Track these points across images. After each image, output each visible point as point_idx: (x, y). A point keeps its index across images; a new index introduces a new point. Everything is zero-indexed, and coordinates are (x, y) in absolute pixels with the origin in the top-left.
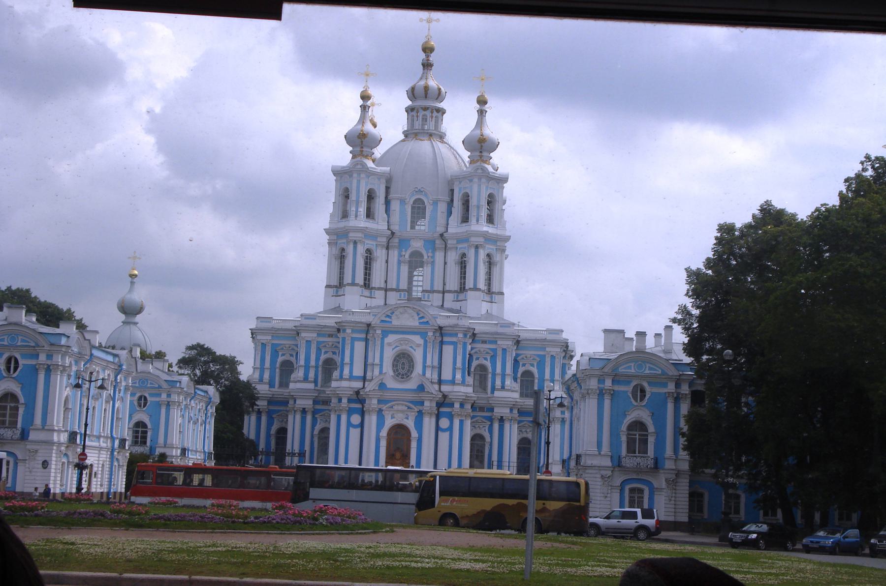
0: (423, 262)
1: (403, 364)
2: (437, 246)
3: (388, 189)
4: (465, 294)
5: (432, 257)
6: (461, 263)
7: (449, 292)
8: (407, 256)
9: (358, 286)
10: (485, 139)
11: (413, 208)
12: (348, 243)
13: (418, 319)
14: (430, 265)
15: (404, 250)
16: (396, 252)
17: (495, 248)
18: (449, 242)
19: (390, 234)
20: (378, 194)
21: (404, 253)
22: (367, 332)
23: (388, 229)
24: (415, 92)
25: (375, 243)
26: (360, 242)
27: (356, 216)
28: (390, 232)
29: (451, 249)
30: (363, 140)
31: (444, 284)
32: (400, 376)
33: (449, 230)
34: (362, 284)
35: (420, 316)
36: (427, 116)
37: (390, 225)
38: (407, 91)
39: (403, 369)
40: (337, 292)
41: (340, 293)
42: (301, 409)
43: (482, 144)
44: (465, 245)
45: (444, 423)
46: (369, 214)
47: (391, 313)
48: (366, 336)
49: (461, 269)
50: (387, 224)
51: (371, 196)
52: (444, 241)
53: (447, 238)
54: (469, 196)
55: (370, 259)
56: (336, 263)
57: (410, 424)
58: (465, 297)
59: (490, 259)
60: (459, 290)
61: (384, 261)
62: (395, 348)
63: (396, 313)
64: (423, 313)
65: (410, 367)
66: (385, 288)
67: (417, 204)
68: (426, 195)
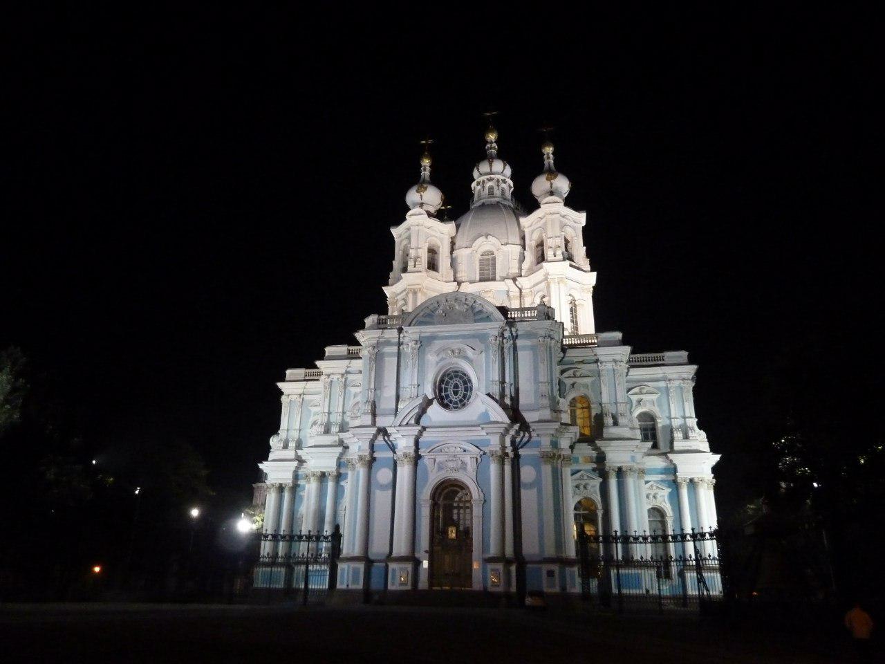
1: (456, 386)
2: (511, 294)
3: (453, 244)
11: (480, 260)
22: (400, 344)
32: (451, 405)
39: (456, 393)
42: (319, 474)
45: (527, 473)
46: (433, 266)
48: (399, 349)
51: (432, 251)
52: (518, 287)
57: (468, 478)
62: (441, 360)
65: (466, 389)
68: (493, 244)
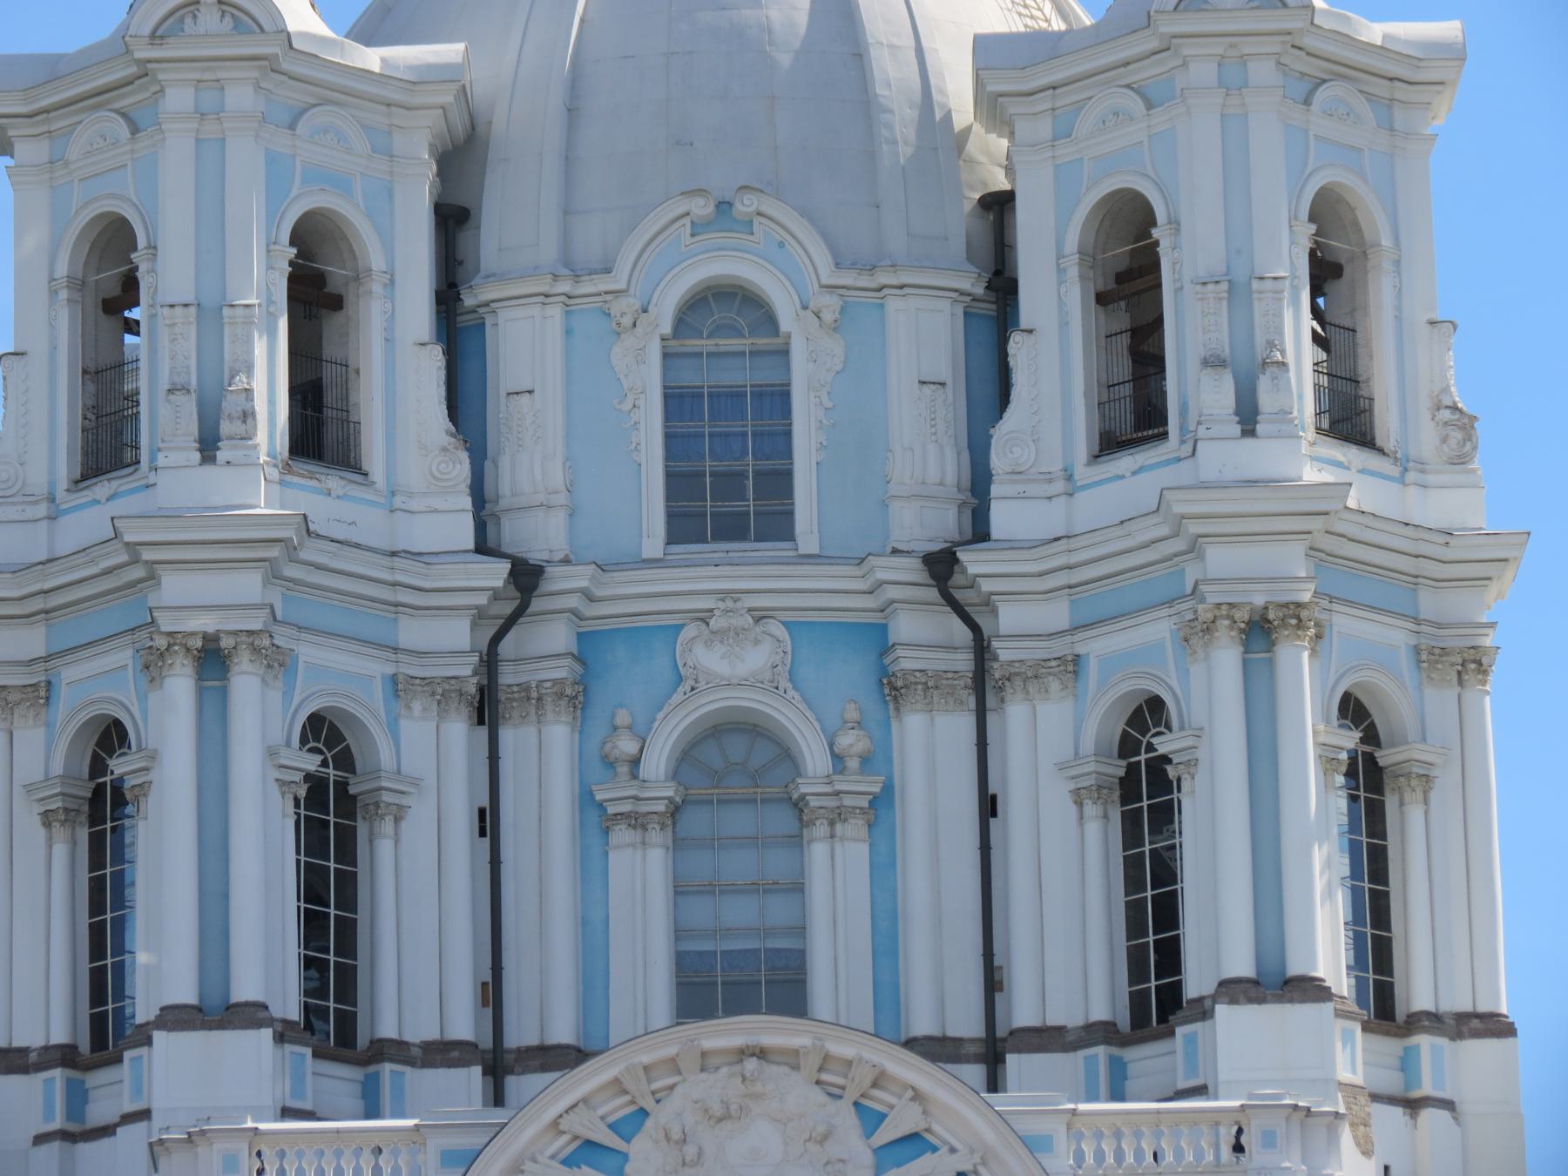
0: (798, 806)
4: (1191, 1040)
5: (865, 760)
6: (1128, 788)
7: (1046, 1038)
8: (657, 762)
9: (258, 1024)
12: (153, 664)
13: (868, 1158)
14: (854, 828)
15: (622, 718)
16: (559, 734)
17: (1397, 636)
18: (1010, 618)
19: (499, 583)
20: (377, 261)
21: (628, 746)
23: (483, 547)
25: (377, 668)
26: (256, 650)
27: (208, 447)
28: (504, 567)
29: (1034, 674)
31: (993, 982)
33: (1002, 518)
34: (294, 1013)
35: (886, 1134)
37: (496, 517)
40: (77, 1099)
41: (100, 1111)
44: (1158, 629)
47: (611, 1127)
49: (1131, 836)
50: (467, 502)
53: (986, 586)
54: (1153, 223)
55: (348, 804)
56: (60, 852)
58: (1192, 1068)
59: (1371, 736)
60: (1124, 1022)
61: (461, 823)
63: (662, 1116)
64: (918, 1096)
66: (487, 1042)
67: (716, 332)
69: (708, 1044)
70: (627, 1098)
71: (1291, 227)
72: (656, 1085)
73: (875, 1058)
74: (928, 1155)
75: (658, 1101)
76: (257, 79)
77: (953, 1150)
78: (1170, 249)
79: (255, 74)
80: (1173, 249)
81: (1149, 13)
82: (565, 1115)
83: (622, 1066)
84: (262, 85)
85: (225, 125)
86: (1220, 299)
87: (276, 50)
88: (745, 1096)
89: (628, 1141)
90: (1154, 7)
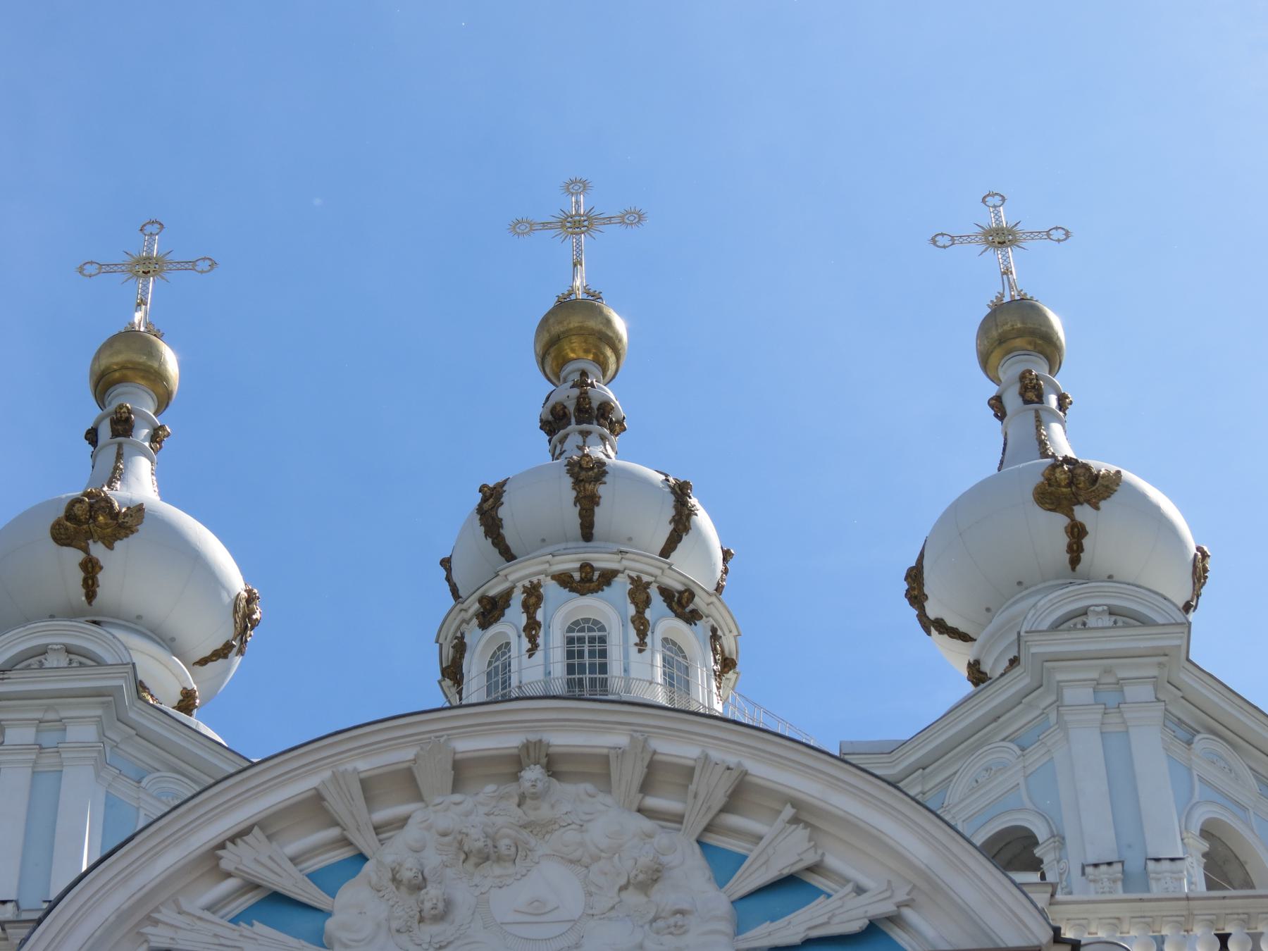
10: (1094, 478)
24: (502, 512)
30: (97, 550)
36: (602, 629)
38: (446, 563)
43: (1083, 513)
47: (312, 877)
69: (466, 746)
70: (334, 832)
71: (1182, 840)
72: (381, 815)
73: (732, 760)
74: (822, 898)
75: (382, 844)
76: (100, 717)
77: (860, 890)
78: (1055, 862)
79: (99, 712)
80: (1058, 862)
81: (1019, 633)
82: (229, 844)
83: (327, 774)
84: (107, 734)
85: (63, 756)
86: (1114, 881)
87: (121, 682)
88: (524, 827)
89: (333, 895)
90: (1023, 630)
